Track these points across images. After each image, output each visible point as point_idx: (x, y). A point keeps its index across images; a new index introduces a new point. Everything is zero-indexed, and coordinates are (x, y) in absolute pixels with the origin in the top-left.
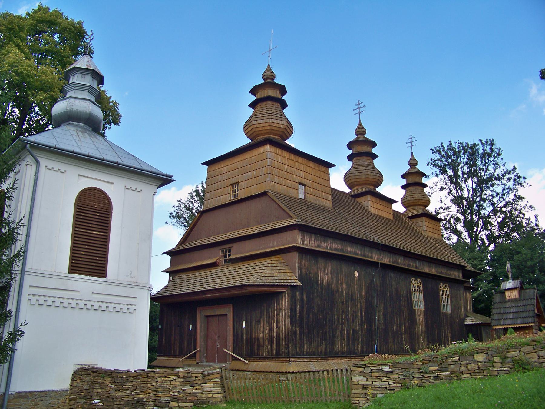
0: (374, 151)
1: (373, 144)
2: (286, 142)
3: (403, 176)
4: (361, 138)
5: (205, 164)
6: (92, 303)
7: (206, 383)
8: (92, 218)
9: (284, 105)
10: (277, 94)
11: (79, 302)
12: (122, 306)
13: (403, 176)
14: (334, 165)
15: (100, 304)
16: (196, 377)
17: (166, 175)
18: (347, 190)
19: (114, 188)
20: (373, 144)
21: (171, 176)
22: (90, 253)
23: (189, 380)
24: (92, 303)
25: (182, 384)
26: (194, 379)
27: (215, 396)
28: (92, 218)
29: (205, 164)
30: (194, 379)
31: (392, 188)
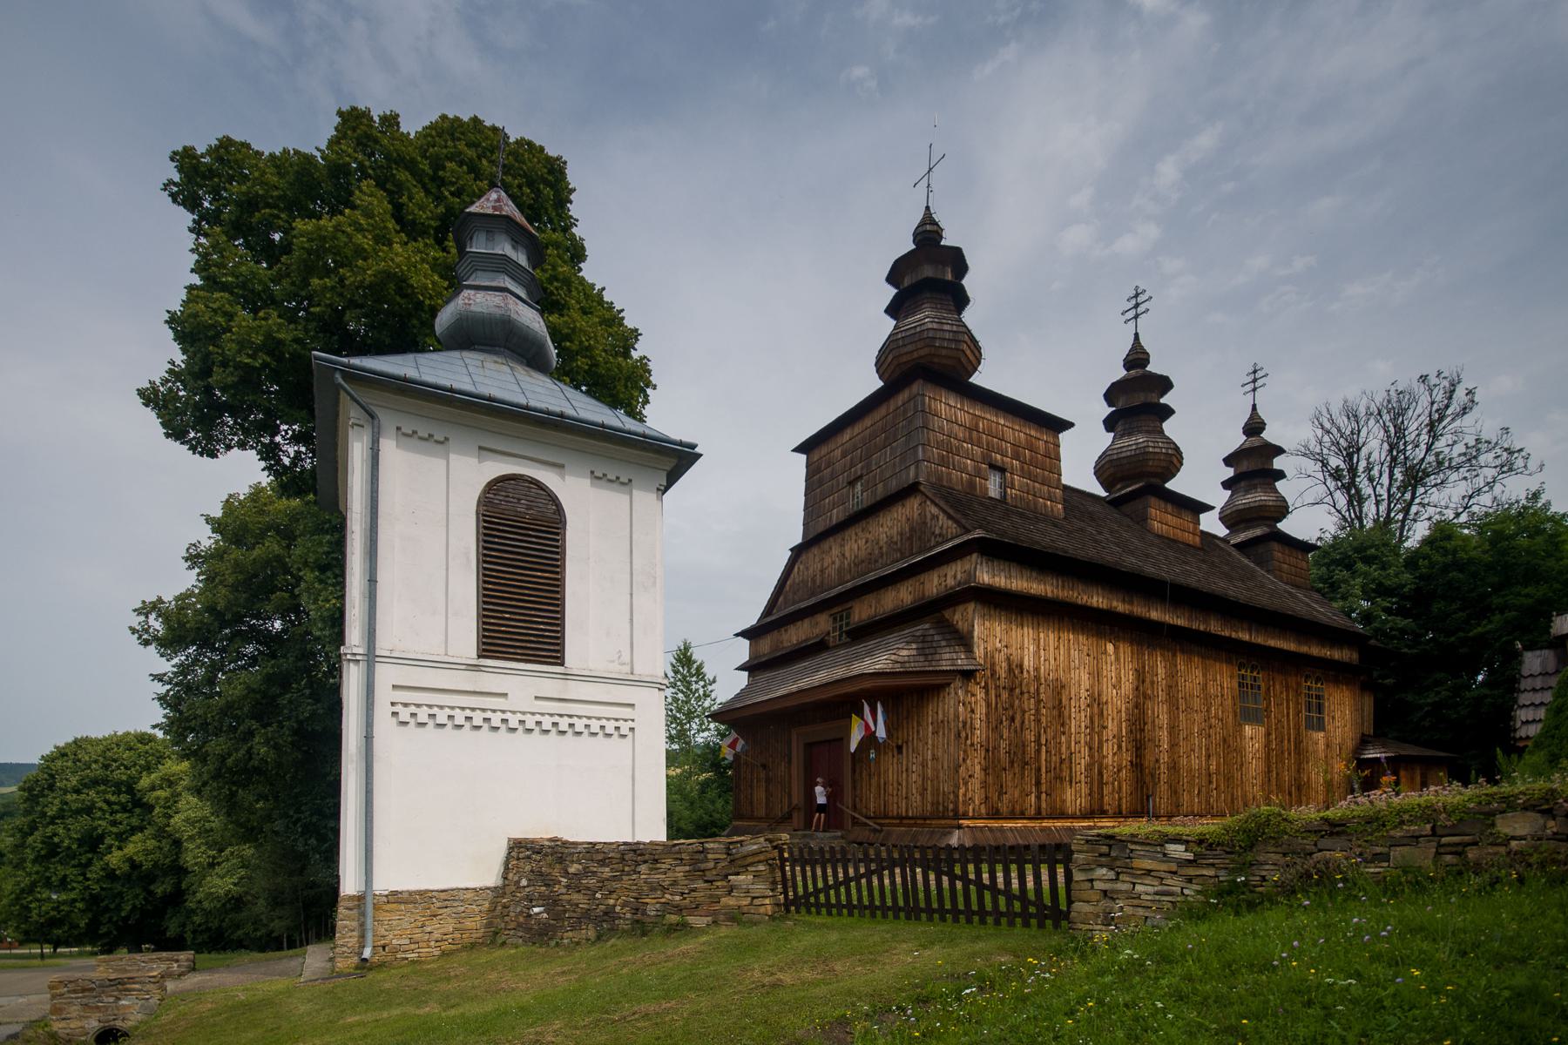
7: (738, 874)
16: (717, 861)
17: (681, 443)
21: (693, 446)
23: (703, 866)
25: (687, 875)
26: (711, 865)
27: (756, 902)
30: (711, 865)
31: (1202, 477)
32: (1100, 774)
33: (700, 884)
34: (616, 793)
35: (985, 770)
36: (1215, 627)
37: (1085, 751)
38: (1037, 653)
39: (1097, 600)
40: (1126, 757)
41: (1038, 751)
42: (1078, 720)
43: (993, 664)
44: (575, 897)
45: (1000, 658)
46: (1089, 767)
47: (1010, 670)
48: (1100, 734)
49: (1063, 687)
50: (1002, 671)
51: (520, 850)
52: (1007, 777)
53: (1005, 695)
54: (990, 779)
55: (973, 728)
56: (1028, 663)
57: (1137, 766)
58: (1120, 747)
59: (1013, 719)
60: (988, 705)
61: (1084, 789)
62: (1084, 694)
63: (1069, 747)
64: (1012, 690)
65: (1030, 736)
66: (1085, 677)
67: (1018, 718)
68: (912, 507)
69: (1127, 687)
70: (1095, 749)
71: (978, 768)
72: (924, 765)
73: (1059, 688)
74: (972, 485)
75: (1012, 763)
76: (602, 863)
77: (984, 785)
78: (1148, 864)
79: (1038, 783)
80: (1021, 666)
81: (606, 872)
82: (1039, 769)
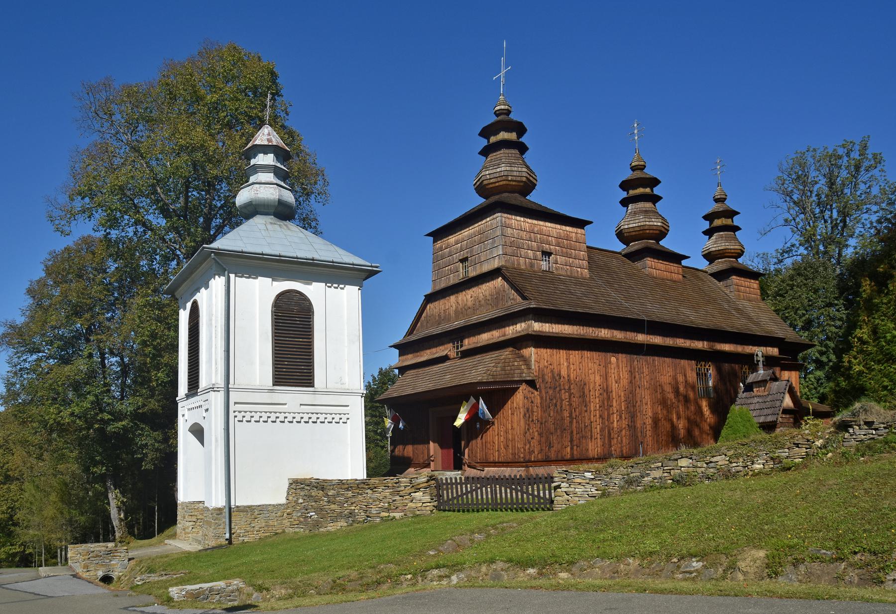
0: (657, 191)
1: (654, 182)
2: (528, 198)
3: (706, 218)
4: (638, 174)
5: (429, 235)
6: (301, 415)
8: (293, 330)
9: (522, 149)
10: (513, 136)
11: (287, 415)
12: (333, 416)
13: (706, 218)
14: (590, 223)
15: (310, 415)
16: (405, 487)
18: (619, 247)
19: (314, 291)
20: (654, 182)
22: (294, 362)
24: (301, 415)
28: (293, 330)
29: (429, 235)
30: (403, 488)
32: (610, 434)
33: (397, 498)
34: (343, 453)
35: (540, 434)
36: (681, 343)
37: (599, 421)
38: (568, 367)
39: (604, 333)
40: (624, 423)
41: (571, 422)
42: (594, 404)
43: (543, 375)
44: (333, 507)
45: (547, 371)
46: (602, 430)
47: (553, 377)
48: (608, 410)
49: (585, 384)
50: (548, 378)
51: (297, 485)
52: (553, 439)
53: (551, 392)
54: (543, 440)
55: (533, 412)
56: (564, 373)
57: (632, 427)
58: (621, 417)
59: (556, 405)
60: (542, 398)
61: (599, 442)
62: (598, 388)
63: (590, 419)
64: (555, 388)
65: (566, 414)
66: (598, 378)
67: (558, 404)
68: (499, 281)
69: (625, 382)
70: (606, 418)
71: (536, 434)
72: (506, 432)
73: (583, 386)
74: (532, 265)
75: (556, 429)
76: (348, 489)
77: (540, 443)
78: (579, 480)
79: (572, 441)
80: (559, 375)
81: (350, 494)
82: (572, 432)
